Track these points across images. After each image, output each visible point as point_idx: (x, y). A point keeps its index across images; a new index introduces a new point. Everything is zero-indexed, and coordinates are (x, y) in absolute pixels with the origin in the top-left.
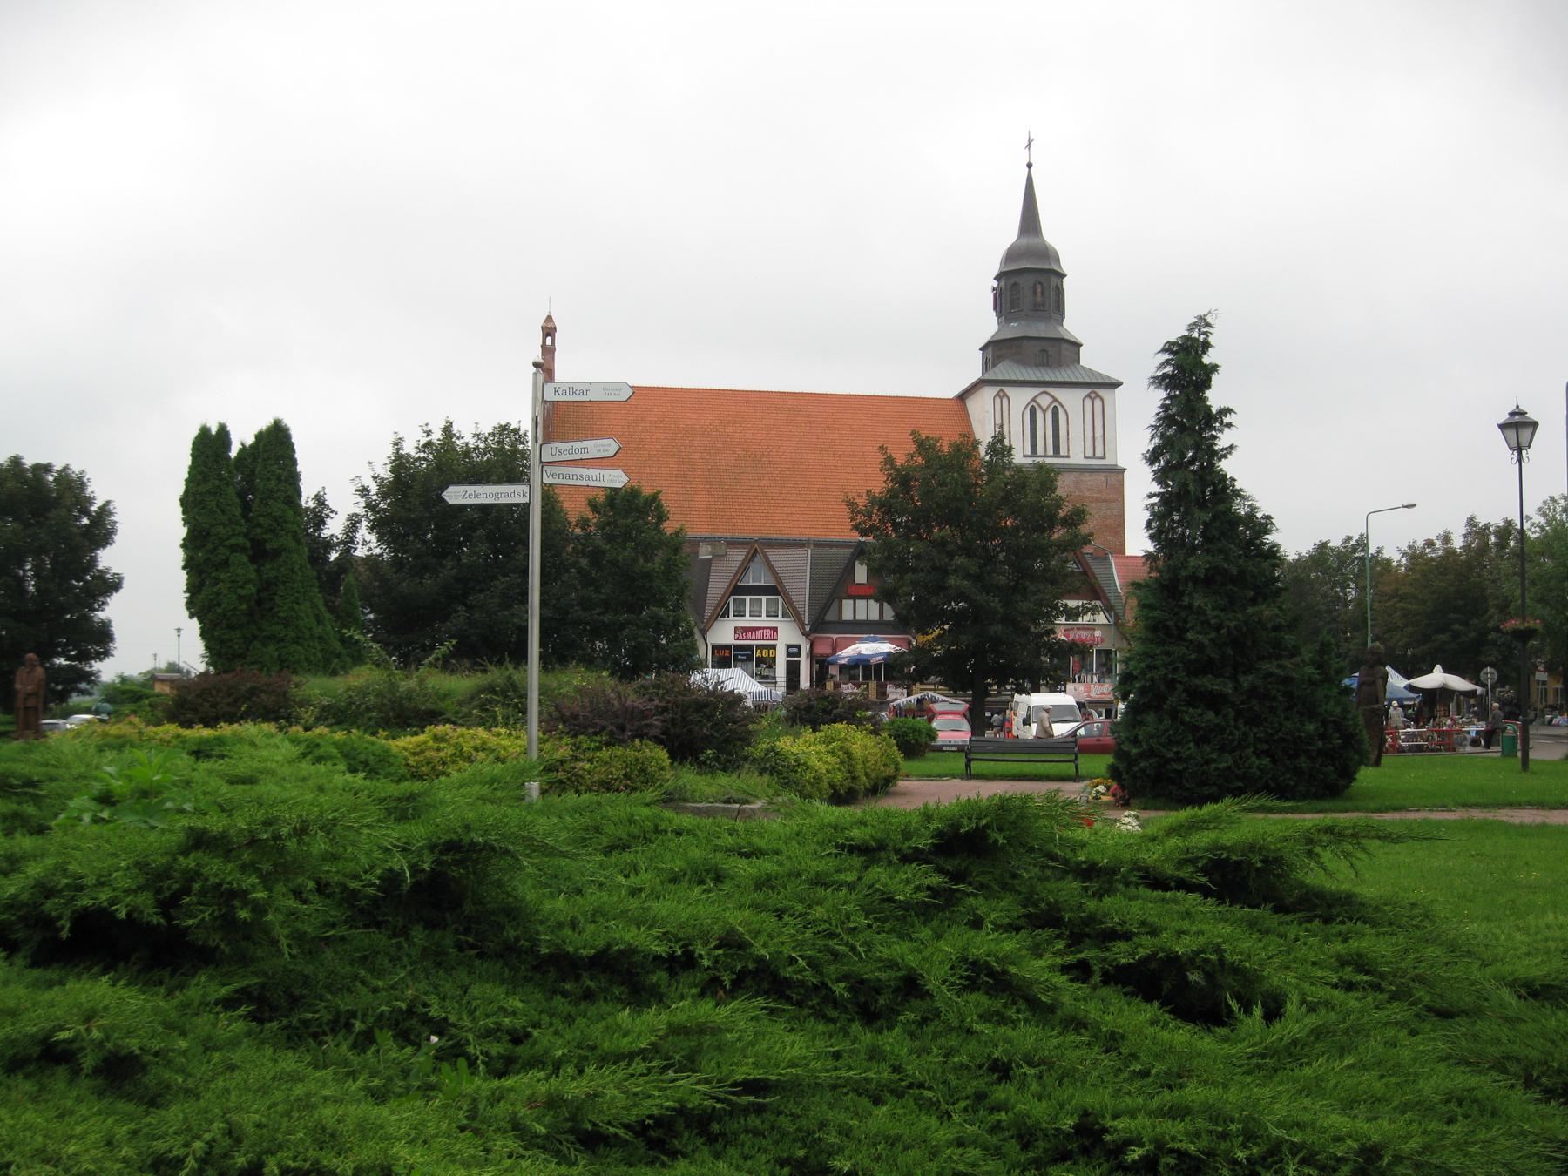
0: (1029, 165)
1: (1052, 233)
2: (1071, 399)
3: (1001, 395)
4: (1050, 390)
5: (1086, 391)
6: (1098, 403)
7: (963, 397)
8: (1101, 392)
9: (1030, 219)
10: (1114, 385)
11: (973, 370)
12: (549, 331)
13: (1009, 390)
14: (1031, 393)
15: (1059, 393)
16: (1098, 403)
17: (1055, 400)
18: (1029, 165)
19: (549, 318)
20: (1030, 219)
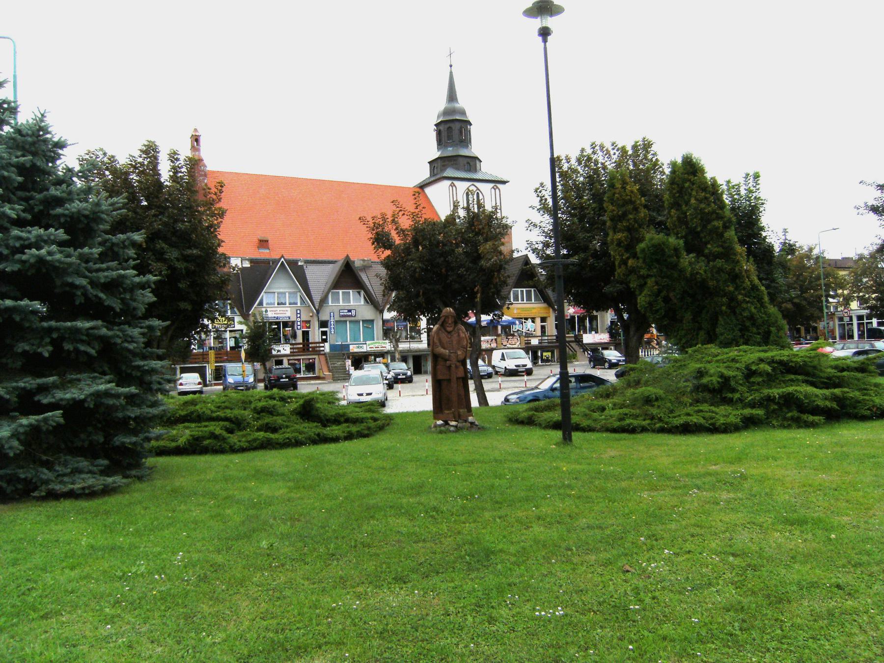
0: (451, 66)
1: (463, 102)
2: (485, 188)
3: (452, 185)
4: (476, 184)
5: (492, 185)
6: (497, 190)
7: (422, 186)
8: (499, 186)
9: (452, 96)
10: (504, 182)
11: (425, 173)
12: (196, 139)
13: (456, 183)
14: (469, 184)
15: (478, 184)
16: (497, 190)
17: (478, 189)
18: (451, 66)
19: (196, 130)
20: (452, 96)
